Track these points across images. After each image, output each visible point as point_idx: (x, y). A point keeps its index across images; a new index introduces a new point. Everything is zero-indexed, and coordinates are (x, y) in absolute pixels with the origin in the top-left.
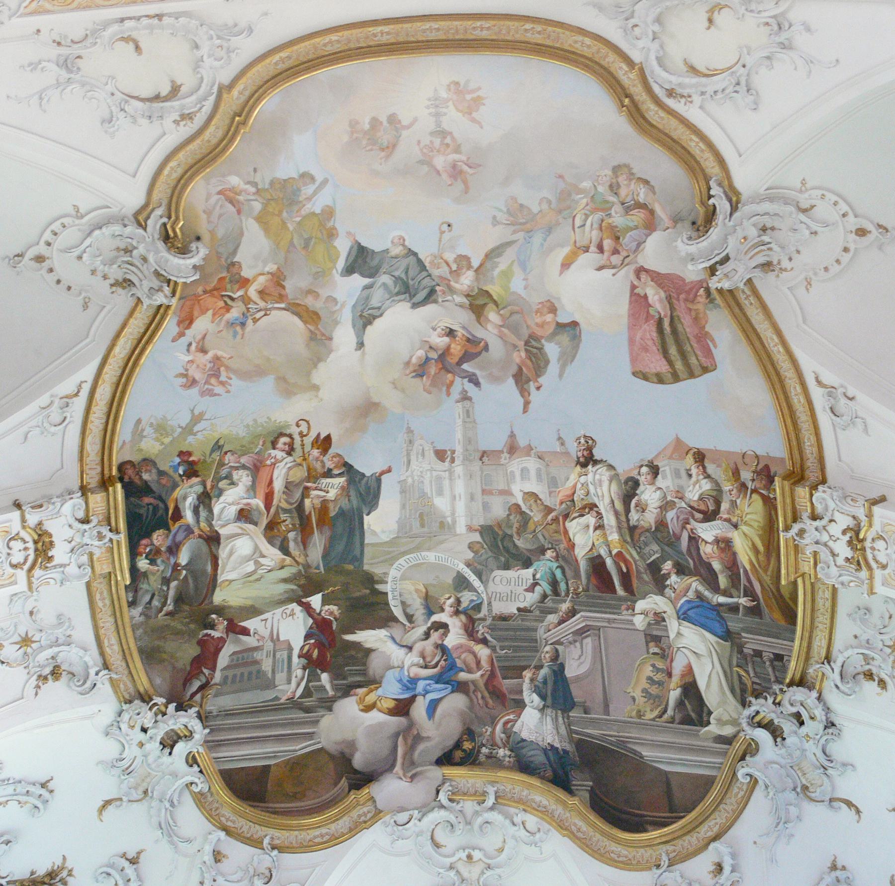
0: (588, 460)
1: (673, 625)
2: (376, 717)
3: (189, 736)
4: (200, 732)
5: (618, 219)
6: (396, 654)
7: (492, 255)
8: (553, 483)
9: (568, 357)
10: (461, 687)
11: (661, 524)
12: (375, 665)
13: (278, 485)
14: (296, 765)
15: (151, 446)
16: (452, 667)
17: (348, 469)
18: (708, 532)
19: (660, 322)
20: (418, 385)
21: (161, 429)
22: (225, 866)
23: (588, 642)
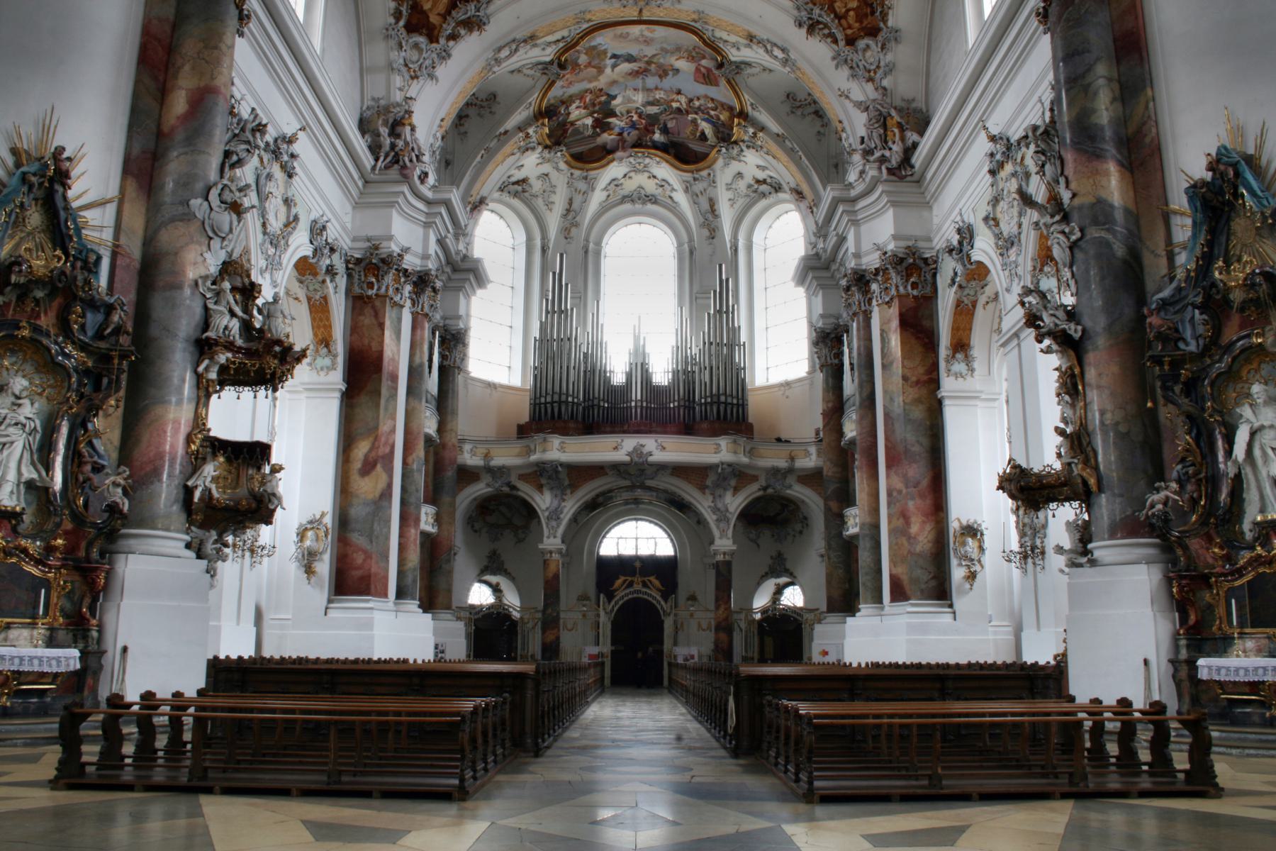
0: (679, 92)
1: (699, 121)
2: (613, 137)
4: (564, 149)
5: (694, 54)
6: (618, 122)
7: (654, 56)
10: (637, 129)
11: (699, 108)
12: (612, 126)
13: (588, 100)
14: (591, 150)
15: (552, 101)
17: (608, 95)
18: (712, 113)
21: (555, 97)
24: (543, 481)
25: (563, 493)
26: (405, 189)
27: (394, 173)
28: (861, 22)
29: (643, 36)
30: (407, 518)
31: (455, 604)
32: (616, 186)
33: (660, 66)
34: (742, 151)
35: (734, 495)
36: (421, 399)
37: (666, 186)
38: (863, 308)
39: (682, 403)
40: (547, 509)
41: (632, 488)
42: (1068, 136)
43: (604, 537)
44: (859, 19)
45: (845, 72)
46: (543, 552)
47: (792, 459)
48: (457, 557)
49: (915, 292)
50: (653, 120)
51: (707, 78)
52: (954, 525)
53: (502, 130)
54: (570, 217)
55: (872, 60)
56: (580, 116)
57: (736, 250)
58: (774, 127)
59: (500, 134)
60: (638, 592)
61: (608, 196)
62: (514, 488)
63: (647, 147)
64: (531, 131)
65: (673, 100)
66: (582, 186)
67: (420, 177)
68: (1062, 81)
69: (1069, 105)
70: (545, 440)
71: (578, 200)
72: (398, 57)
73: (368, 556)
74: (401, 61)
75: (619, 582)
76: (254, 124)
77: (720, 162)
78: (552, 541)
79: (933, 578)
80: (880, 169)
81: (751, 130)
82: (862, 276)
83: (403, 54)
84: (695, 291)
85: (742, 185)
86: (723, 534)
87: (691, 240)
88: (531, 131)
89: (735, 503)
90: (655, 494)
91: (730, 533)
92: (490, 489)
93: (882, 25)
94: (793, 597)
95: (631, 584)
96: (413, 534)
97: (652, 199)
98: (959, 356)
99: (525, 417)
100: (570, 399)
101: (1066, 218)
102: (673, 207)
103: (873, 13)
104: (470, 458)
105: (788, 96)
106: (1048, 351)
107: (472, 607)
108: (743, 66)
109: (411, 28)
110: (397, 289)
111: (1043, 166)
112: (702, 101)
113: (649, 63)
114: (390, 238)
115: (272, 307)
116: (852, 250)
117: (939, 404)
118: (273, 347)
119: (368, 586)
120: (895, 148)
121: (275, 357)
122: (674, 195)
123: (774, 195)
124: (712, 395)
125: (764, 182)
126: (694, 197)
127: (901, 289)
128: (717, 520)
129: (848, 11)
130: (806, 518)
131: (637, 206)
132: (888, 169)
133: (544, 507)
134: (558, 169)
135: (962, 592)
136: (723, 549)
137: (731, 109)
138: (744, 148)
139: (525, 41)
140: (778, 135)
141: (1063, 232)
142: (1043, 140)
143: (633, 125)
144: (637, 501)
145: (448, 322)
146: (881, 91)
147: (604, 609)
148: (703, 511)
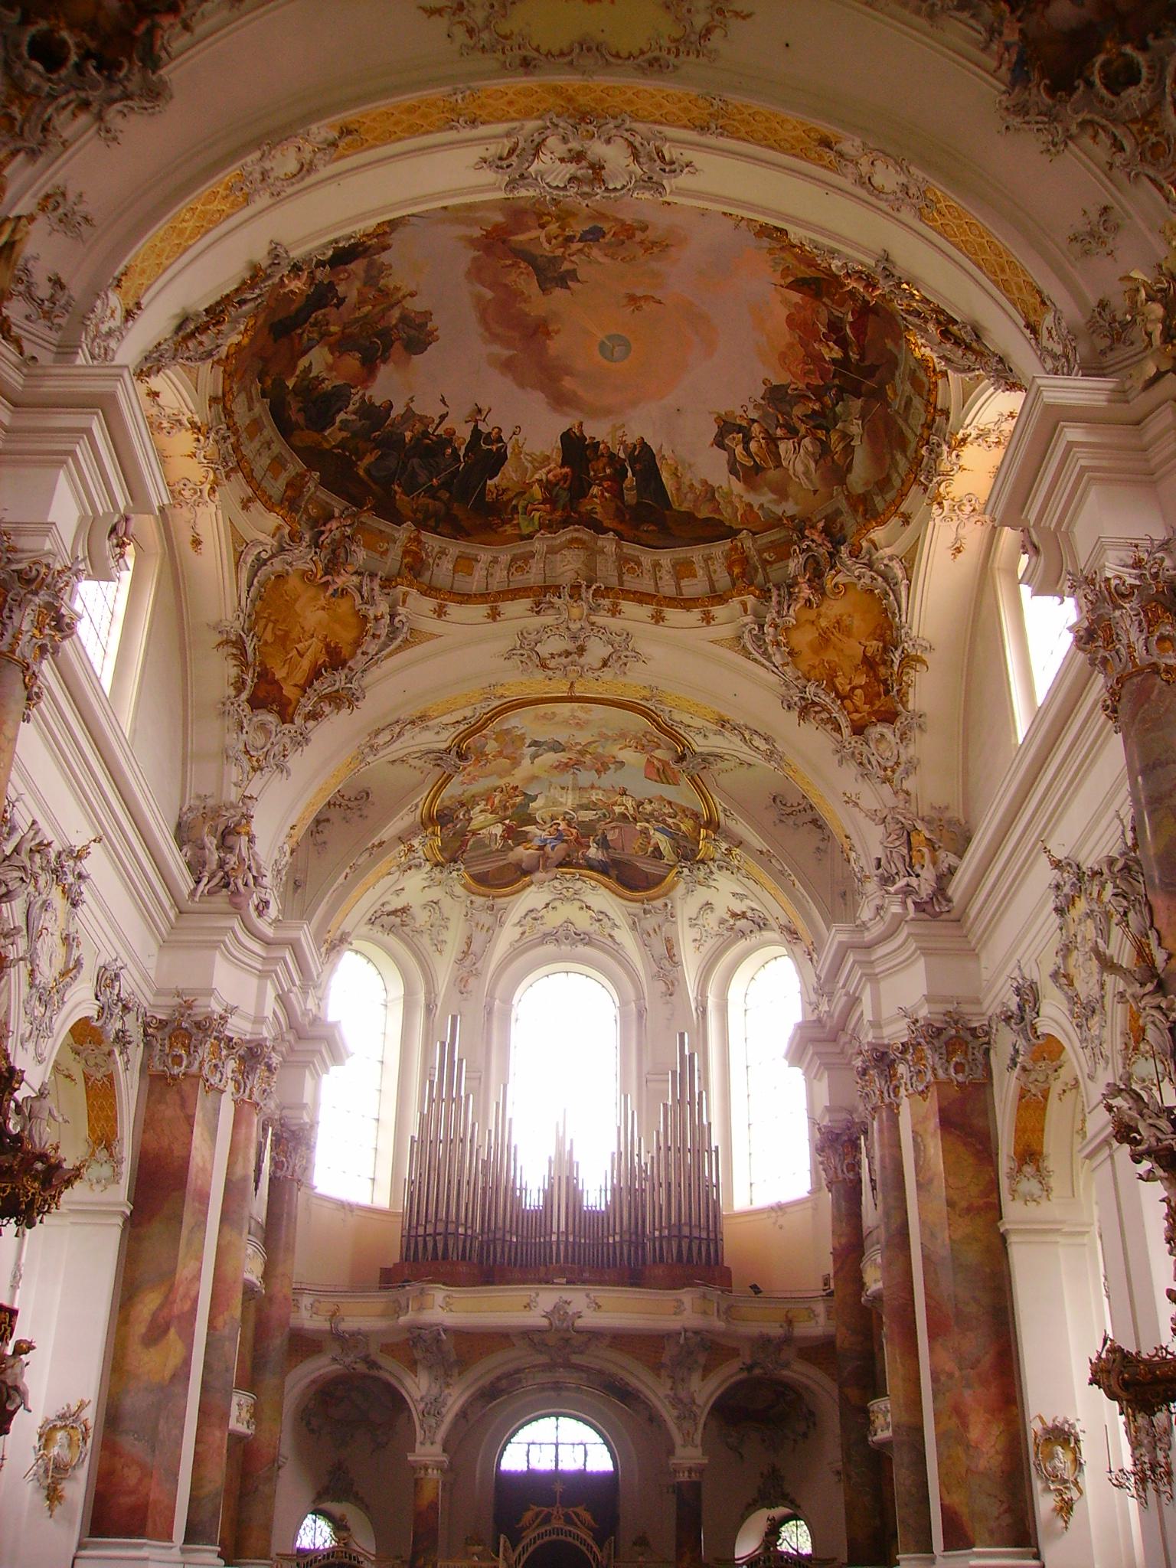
0: (624, 793)
1: (652, 832)
3: (459, 870)
4: (462, 867)
5: (644, 741)
8: (609, 798)
9: (616, 770)
11: (651, 814)
13: (496, 801)
14: (500, 869)
15: (447, 803)
16: (561, 835)
18: (670, 821)
19: (658, 770)
20: (555, 771)
21: (451, 798)
22: (475, 906)
23: (617, 830)
24: (418, 1354)
25: (447, 1375)
26: (236, 924)
27: (221, 900)
28: (872, 704)
29: (574, 717)
30: (211, 1412)
31: (276, 1548)
32: (535, 919)
33: (597, 757)
34: (711, 872)
35: (704, 1378)
36: (241, 1234)
37: (605, 920)
38: (887, 1100)
39: (626, 1237)
40: (422, 1398)
41: (551, 1367)
42: (1156, 874)
43: (508, 1441)
44: (869, 701)
45: (852, 769)
46: (413, 1468)
47: (790, 1322)
48: (281, 1473)
49: (960, 1077)
50: (587, 830)
51: (662, 774)
52: (1034, 1427)
53: (376, 840)
54: (467, 963)
55: (888, 754)
56: (486, 824)
57: (704, 1012)
58: (756, 841)
59: (373, 846)
60: (558, 1531)
61: (523, 933)
62: (373, 1364)
63: (579, 866)
64: (416, 842)
65: (615, 804)
66: (486, 918)
67: (257, 907)
68: (1143, 800)
69: (1154, 833)
70: (422, 1292)
71: (479, 937)
72: (236, 742)
73: (146, 1472)
74: (241, 747)
75: (529, 1515)
76: (33, 843)
77: (681, 888)
78: (428, 1451)
79: (1006, 1512)
80: (904, 903)
81: (724, 846)
82: (884, 1054)
83: (245, 736)
84: (645, 1070)
85: (711, 920)
86: (688, 1437)
87: (640, 997)
88: (416, 842)
89: (704, 1390)
90: (584, 1375)
91: (698, 1438)
92: (338, 1367)
93: (900, 707)
94: (797, 1539)
95: (547, 1520)
96: (218, 1438)
97: (584, 938)
98: (1028, 1169)
99: (395, 1257)
100: (461, 1230)
101: (1161, 988)
102: (615, 951)
103: (887, 692)
104: (309, 1318)
105: (774, 799)
106: (1148, 1177)
107: (302, 1552)
108: (712, 759)
109: (255, 703)
110: (216, 1066)
111: (1125, 914)
112: (655, 805)
113: (582, 753)
114: (210, 992)
115: (37, 1104)
116: (868, 1016)
117: (1003, 1238)
118: (32, 1164)
119: (144, 1519)
120: (924, 874)
121: (35, 1178)
122: (616, 933)
123: (757, 934)
124: (669, 1226)
125: (743, 915)
126: (645, 938)
127: (940, 1072)
128: (678, 1418)
129: (853, 689)
130: (812, 1413)
131: (563, 947)
132: (915, 903)
133: (417, 1396)
134: (452, 895)
135: (1054, 1535)
136: (688, 1463)
137: (696, 816)
138: (714, 869)
139: (413, 722)
140: (761, 852)
141: (1159, 1008)
142: (1123, 879)
143: (559, 837)
144: (557, 1387)
145: (286, 1112)
146: (902, 796)
147: (506, 1559)
148: (658, 1404)
